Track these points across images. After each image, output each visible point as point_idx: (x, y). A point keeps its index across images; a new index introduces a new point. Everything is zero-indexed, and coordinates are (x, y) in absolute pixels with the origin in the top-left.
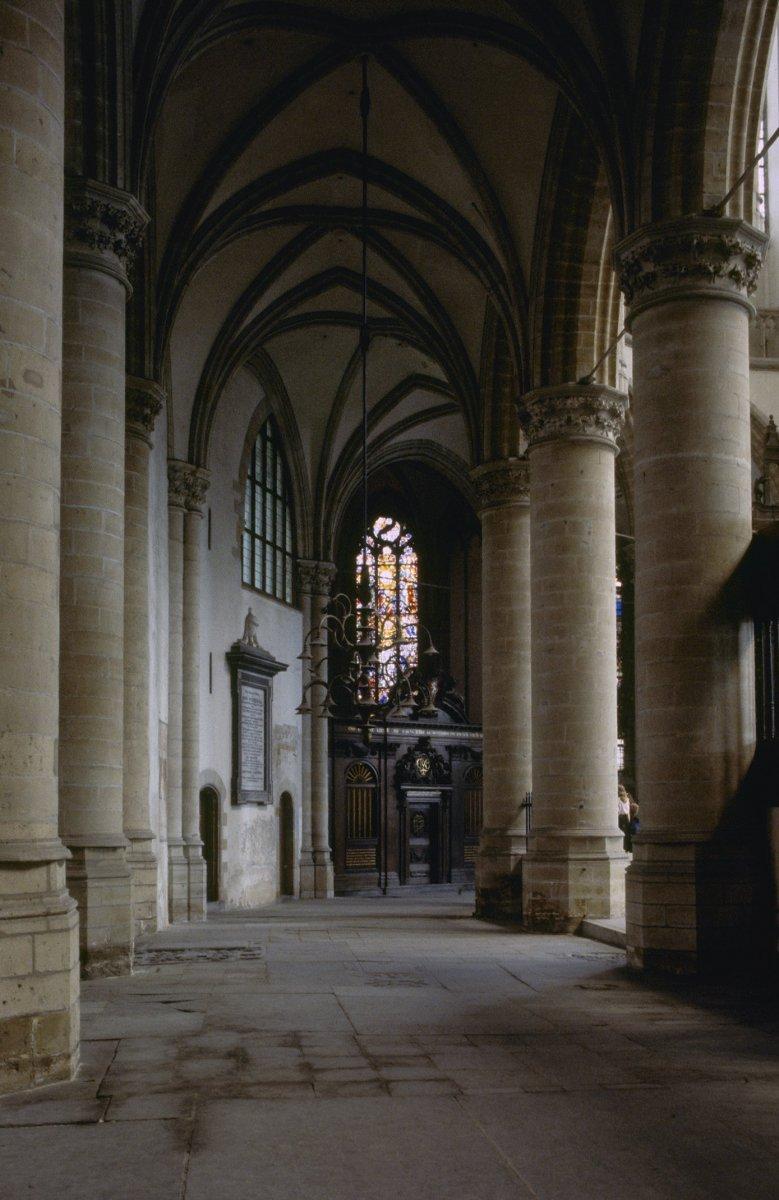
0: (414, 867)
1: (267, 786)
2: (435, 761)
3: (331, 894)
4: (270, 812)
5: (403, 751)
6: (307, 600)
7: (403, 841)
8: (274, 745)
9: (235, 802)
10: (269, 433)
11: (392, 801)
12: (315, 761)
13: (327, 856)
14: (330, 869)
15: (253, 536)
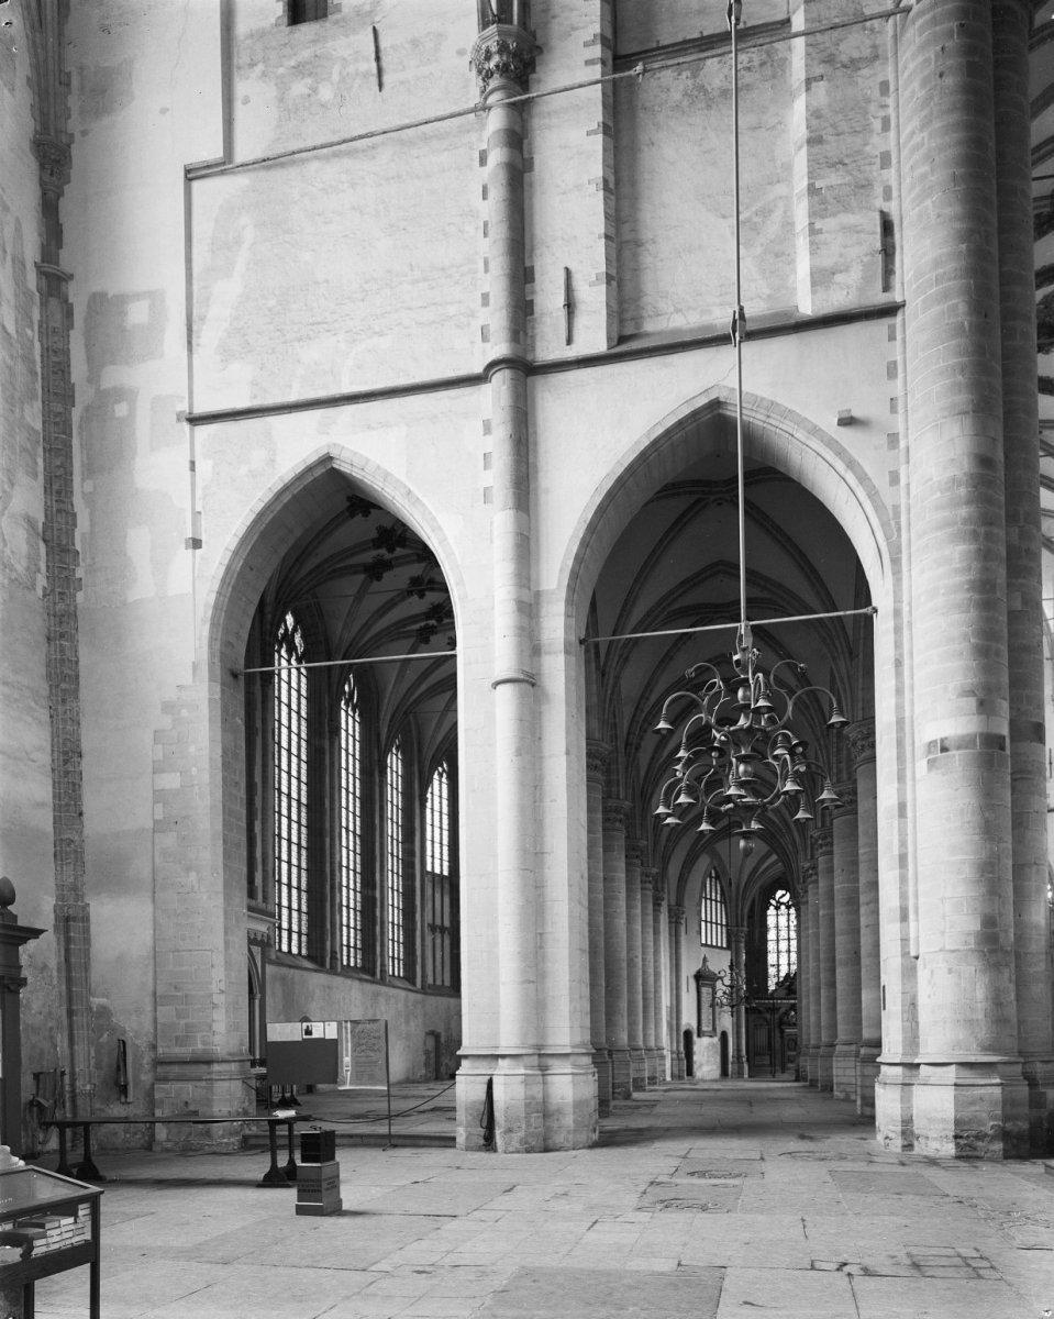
3: (746, 1076)
4: (716, 1040)
5: (783, 1010)
6: (733, 946)
9: (699, 1036)
11: (778, 1034)
14: (746, 1066)
15: (706, 921)
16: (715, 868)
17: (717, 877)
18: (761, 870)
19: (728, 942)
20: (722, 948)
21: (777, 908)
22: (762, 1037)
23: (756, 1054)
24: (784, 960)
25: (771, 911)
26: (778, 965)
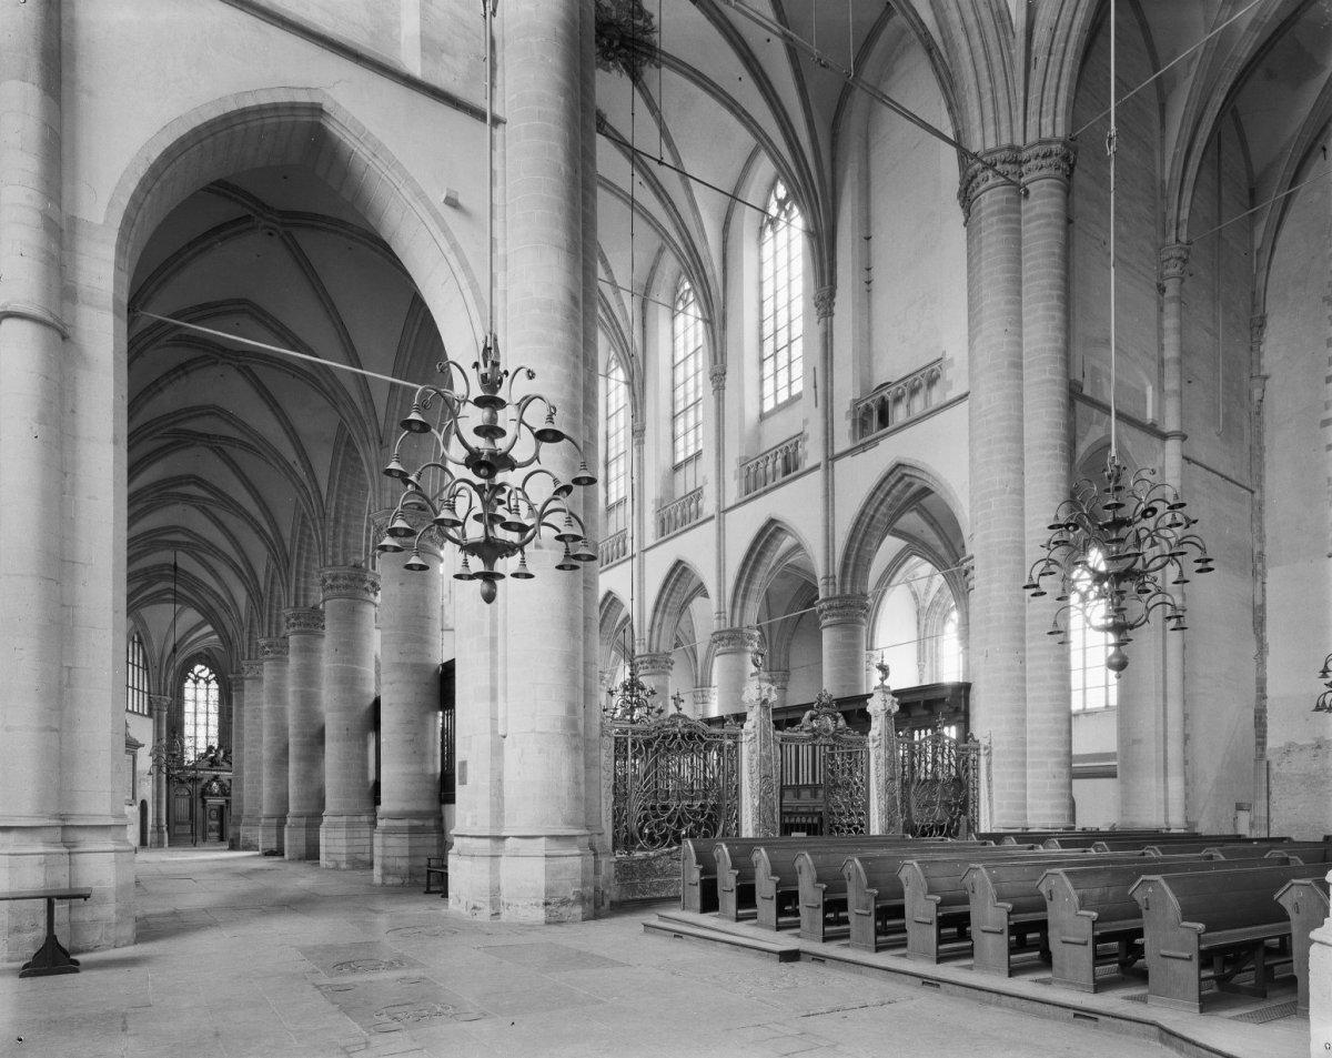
0: (211, 834)
1: (134, 797)
2: (222, 786)
4: (136, 809)
5: (205, 781)
6: (155, 713)
7: (204, 822)
8: (138, 779)
10: (136, 639)
11: (199, 804)
12: (159, 787)
13: (165, 829)
14: (166, 835)
16: (138, 633)
17: (140, 642)
18: (189, 641)
19: (150, 709)
20: (143, 715)
21: (196, 682)
22: (182, 806)
23: (177, 823)
24: (201, 732)
25: (189, 684)
26: (196, 737)
